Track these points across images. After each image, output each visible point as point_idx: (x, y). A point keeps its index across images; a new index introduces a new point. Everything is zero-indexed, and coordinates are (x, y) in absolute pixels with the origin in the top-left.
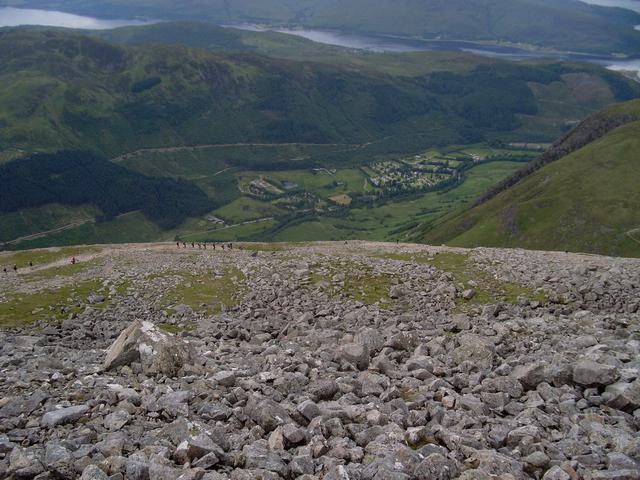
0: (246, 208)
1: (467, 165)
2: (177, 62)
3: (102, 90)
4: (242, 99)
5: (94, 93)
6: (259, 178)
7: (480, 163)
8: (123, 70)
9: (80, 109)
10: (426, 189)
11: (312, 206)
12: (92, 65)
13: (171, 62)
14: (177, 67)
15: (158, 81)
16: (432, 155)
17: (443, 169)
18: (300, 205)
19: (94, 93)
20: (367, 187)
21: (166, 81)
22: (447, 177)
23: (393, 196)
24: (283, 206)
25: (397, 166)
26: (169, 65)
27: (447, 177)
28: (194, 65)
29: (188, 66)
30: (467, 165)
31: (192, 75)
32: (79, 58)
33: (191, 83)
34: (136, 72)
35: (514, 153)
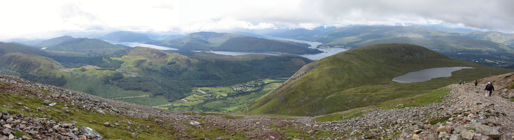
0: (194, 97)
1: (263, 85)
7: (268, 84)
10: (251, 92)
11: (215, 97)
12: (157, 56)
16: (252, 82)
17: (256, 86)
18: (211, 97)
20: (232, 91)
22: (258, 88)
23: (240, 94)
24: (206, 97)
25: (241, 85)
27: (258, 88)
30: (263, 85)
32: (154, 54)
35: (278, 81)
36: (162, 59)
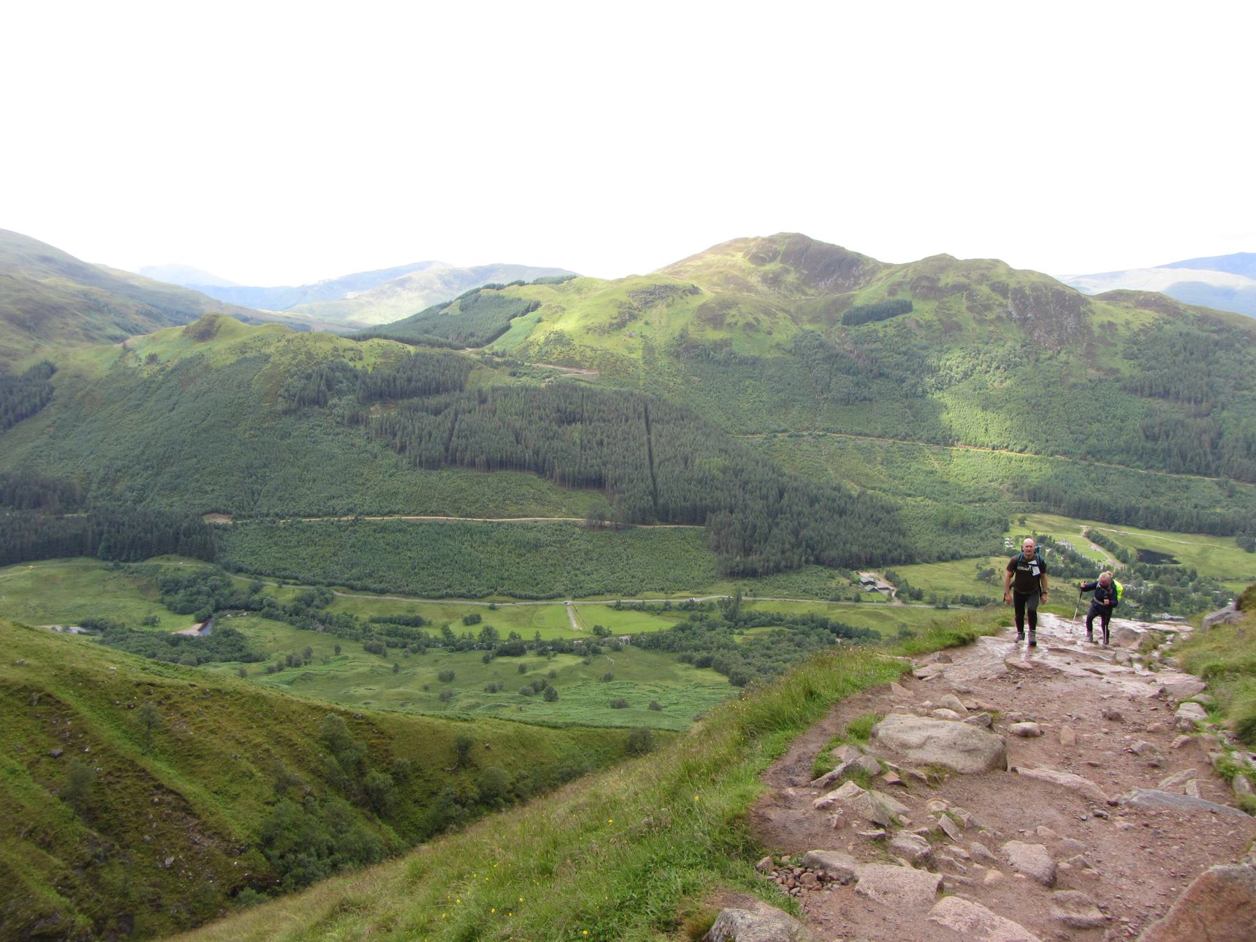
2: (963, 280)
3: (780, 315)
4: (1098, 369)
5: (761, 316)
6: (1078, 531)
8: (849, 288)
9: (713, 335)
13: (948, 279)
14: (958, 288)
15: (906, 308)
19: (761, 316)
21: (925, 310)
26: (942, 284)
28: (1001, 289)
29: (984, 289)
31: (987, 308)
33: (981, 322)
34: (864, 296)
36: (818, 296)
